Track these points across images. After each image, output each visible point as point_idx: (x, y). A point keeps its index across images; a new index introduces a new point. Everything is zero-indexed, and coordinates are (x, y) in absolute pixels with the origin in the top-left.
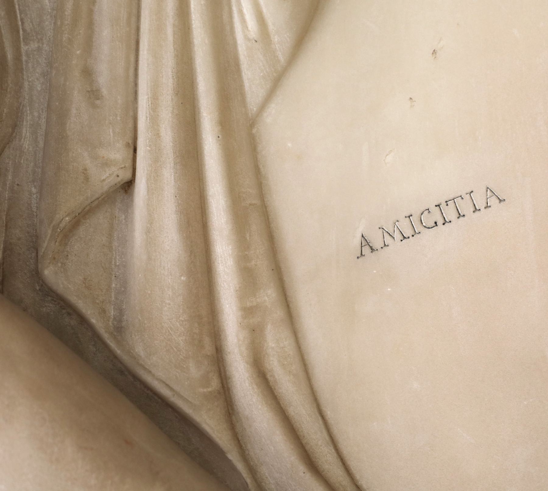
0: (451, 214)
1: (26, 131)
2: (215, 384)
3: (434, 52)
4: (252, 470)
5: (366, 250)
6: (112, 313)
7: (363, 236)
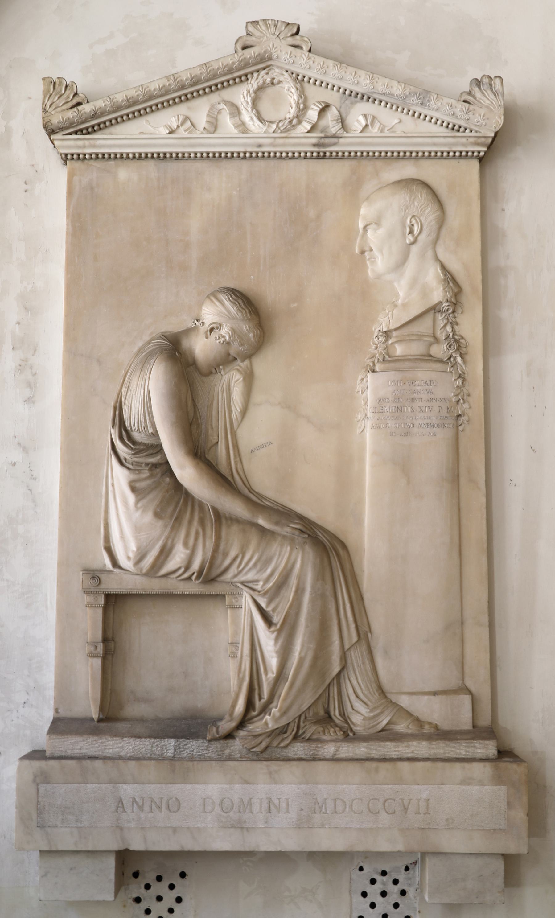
1: (202, 434)
2: (231, 473)
4: (236, 486)
6: (216, 462)
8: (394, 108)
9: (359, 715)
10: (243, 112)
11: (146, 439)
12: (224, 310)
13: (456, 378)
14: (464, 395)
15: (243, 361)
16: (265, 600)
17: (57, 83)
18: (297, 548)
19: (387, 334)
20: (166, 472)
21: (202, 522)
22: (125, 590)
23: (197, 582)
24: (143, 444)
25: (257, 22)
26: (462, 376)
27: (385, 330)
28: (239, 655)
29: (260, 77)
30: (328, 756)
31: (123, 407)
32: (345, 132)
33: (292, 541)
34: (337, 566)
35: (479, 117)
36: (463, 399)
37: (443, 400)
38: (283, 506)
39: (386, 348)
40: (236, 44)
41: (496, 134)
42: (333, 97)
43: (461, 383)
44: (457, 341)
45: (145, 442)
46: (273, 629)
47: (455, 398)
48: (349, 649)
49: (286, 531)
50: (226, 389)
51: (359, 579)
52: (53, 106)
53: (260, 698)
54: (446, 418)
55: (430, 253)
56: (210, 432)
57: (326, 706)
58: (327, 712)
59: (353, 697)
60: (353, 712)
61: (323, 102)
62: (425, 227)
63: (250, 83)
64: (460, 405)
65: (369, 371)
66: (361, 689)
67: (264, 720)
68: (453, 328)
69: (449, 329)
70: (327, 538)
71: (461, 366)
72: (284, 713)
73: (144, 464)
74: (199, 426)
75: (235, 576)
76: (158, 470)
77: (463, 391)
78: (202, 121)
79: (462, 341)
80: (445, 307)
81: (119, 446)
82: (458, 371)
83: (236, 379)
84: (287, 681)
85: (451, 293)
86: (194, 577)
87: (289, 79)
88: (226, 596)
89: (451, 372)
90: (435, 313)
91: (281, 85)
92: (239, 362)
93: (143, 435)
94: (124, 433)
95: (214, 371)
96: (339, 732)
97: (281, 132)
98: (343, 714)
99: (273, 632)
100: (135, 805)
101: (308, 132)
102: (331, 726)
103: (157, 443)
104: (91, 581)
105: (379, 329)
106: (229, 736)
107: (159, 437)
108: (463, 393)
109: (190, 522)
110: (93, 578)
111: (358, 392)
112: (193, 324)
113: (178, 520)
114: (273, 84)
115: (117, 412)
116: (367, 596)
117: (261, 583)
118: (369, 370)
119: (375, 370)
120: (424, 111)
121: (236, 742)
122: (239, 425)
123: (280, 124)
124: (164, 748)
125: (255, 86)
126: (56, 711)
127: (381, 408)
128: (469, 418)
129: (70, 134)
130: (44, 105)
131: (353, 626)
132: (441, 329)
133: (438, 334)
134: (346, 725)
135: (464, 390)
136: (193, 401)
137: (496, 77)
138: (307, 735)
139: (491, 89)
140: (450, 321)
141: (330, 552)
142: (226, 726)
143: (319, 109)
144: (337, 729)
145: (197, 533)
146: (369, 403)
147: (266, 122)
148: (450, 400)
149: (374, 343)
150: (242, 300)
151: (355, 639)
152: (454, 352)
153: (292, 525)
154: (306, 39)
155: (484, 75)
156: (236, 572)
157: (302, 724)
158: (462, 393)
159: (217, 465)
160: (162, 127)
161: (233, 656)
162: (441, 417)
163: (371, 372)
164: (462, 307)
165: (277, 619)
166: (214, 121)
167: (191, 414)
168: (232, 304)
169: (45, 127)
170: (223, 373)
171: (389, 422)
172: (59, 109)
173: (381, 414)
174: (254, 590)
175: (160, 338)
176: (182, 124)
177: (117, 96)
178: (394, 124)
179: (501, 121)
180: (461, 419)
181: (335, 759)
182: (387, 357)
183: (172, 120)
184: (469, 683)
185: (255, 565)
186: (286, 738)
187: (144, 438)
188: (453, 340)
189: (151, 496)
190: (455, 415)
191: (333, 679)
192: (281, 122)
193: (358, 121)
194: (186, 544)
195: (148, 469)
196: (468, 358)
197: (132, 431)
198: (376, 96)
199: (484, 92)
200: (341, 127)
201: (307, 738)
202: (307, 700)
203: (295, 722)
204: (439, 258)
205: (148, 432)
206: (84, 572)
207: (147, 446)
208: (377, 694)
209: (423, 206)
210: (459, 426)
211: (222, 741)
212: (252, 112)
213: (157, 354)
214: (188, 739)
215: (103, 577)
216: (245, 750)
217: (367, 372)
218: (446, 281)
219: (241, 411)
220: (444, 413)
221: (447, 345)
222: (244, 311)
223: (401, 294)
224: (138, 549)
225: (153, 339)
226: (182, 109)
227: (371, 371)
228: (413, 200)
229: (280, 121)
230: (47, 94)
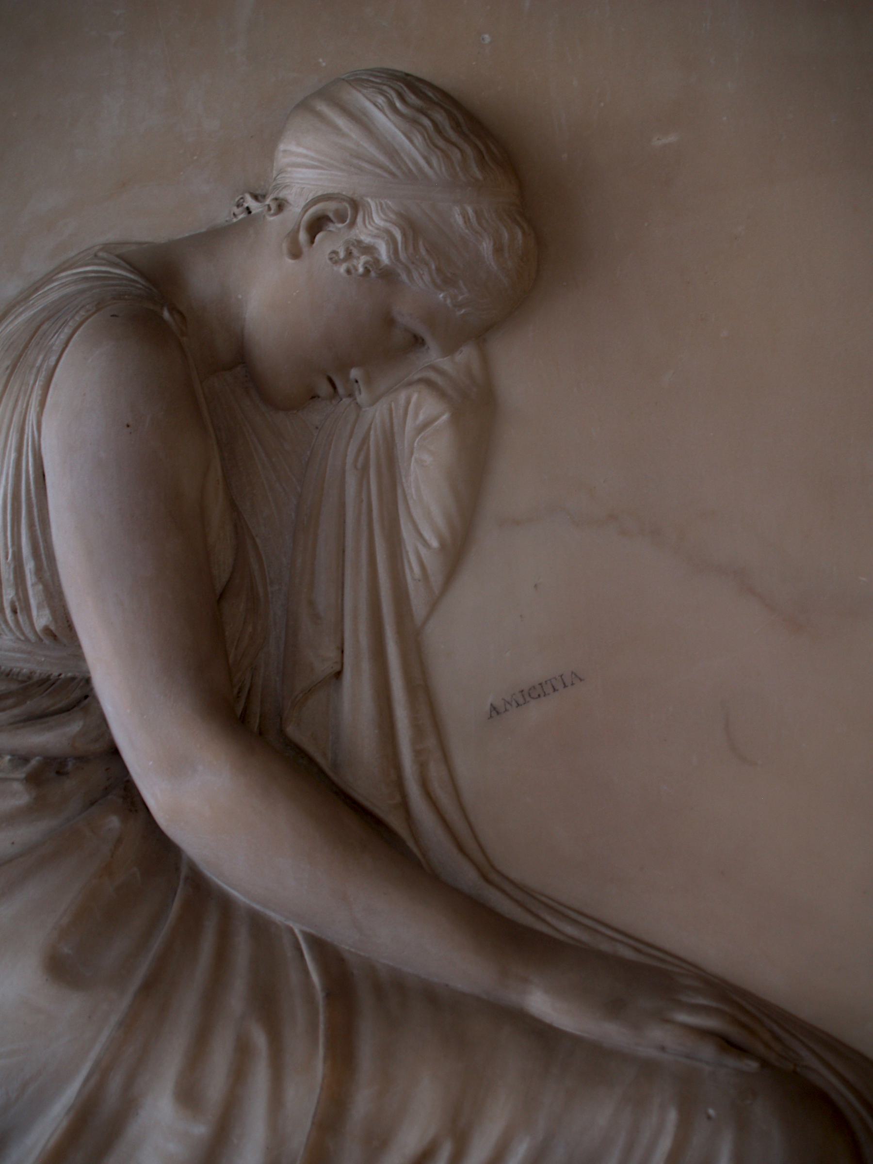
0: (548, 689)
3: (536, 586)
5: (494, 713)
7: (491, 705)
11: (18, 655)
12: (370, 148)
15: (449, 350)
18: (709, 1117)
20: (107, 791)
24: (8, 675)
45: (16, 670)
73: (8, 758)
76: (69, 784)
83: (421, 417)
92: (433, 355)
95: (324, 388)
103: (69, 675)
107: (79, 647)
112: (236, 210)
122: (434, 606)
136: (233, 506)
153: (683, 1017)
170: (363, 397)
187: (13, 650)
195: (23, 776)
205: (32, 625)
213: (82, 313)
219: (443, 545)
222: (456, 151)
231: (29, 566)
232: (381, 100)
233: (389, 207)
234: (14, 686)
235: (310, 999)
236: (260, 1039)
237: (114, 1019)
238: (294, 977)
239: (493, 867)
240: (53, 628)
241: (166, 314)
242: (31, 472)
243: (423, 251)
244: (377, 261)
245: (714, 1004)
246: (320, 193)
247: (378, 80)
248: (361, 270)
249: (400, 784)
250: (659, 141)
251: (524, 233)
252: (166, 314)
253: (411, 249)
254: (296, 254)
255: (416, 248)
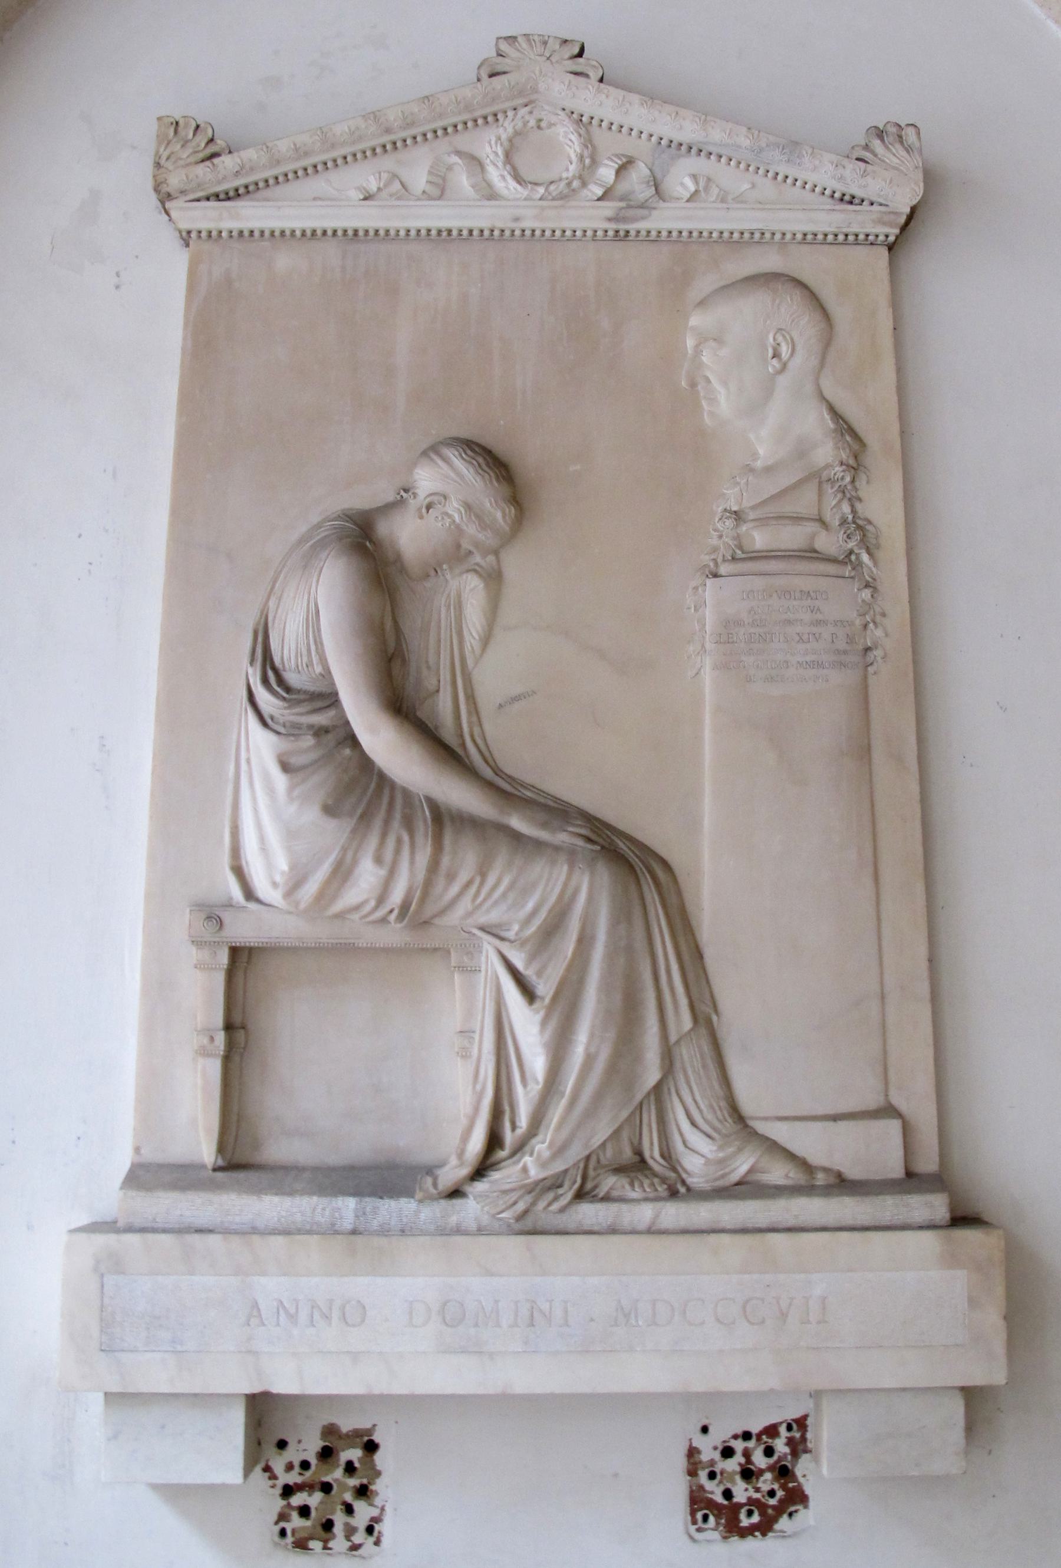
0: (522, 698)
8: (742, 166)
9: (696, 1155)
10: (490, 169)
11: (308, 684)
13: (861, 587)
14: (874, 615)
16: (523, 955)
17: (181, 123)
18: (580, 868)
19: (738, 516)
21: (409, 824)
22: (266, 940)
23: (399, 926)
25: (515, 38)
26: (871, 585)
27: (735, 508)
28: (475, 1052)
29: (519, 116)
30: (642, 1226)
31: (270, 631)
32: (661, 201)
33: (572, 854)
34: (653, 898)
35: (884, 183)
36: (875, 623)
37: (839, 624)
38: (556, 799)
39: (738, 538)
40: (479, 68)
41: (913, 210)
42: (641, 148)
43: (869, 595)
44: (860, 528)
45: (308, 690)
46: (537, 1005)
47: (861, 620)
48: (678, 1042)
49: (562, 838)
50: (454, 601)
51: (694, 923)
52: (173, 159)
53: (514, 1127)
54: (845, 652)
55: (809, 388)
56: (425, 672)
57: (636, 1142)
58: (639, 1153)
59: (685, 1125)
60: (687, 1151)
61: (623, 155)
62: (799, 348)
63: (502, 126)
64: (868, 632)
65: (707, 576)
66: (701, 1111)
67: (521, 1165)
68: (852, 506)
69: (846, 508)
70: (638, 853)
71: (870, 569)
72: (559, 1151)
74: (404, 662)
75: (469, 914)
76: (330, 736)
77: (873, 608)
78: (419, 179)
79: (869, 527)
80: (838, 474)
81: (263, 696)
82: (864, 576)
83: (472, 585)
84: (563, 1097)
85: (848, 450)
86: (393, 917)
87: (567, 120)
88: (452, 950)
89: (852, 578)
90: (820, 483)
91: (553, 128)
93: (304, 678)
94: (271, 674)
95: (432, 573)
96: (661, 1186)
97: (553, 199)
98: (667, 1155)
99: (537, 1012)
100: (282, 1312)
101: (599, 199)
102: (646, 1177)
104: (205, 924)
105: (725, 507)
106: (456, 1193)
108: (874, 611)
109: (387, 822)
110: (209, 918)
111: (689, 608)
113: (365, 818)
114: (539, 127)
115: (260, 639)
116: (709, 953)
117: (516, 927)
118: (707, 573)
119: (719, 574)
120: (792, 173)
121: (469, 1201)
122: (476, 663)
123: (552, 187)
124: (336, 1213)
125: (510, 130)
126: (137, 1150)
127: (730, 636)
128: (885, 653)
129: (198, 200)
130: (158, 158)
131: (684, 1002)
132: (832, 509)
133: (828, 516)
134: (673, 1175)
135: (876, 607)
137: (908, 125)
138: (602, 1191)
139: (902, 143)
140: (848, 495)
141: (640, 874)
142: (453, 1173)
143: (616, 166)
144: (656, 1181)
145: (399, 841)
146: (708, 628)
147: (529, 184)
148: (851, 624)
149: (715, 530)
150: (485, 459)
151: (687, 1023)
152: (857, 545)
153: (571, 829)
154: (594, 63)
155: (888, 122)
156: (470, 907)
157: (591, 1173)
158: (872, 612)
159: (436, 728)
160: (354, 190)
161: (464, 1054)
162: (836, 652)
163: (711, 577)
164: (868, 474)
165: (545, 989)
166: (441, 182)
167: (392, 644)
168: (467, 465)
169: (157, 189)
171: (743, 658)
172: (181, 162)
173: (728, 645)
174: (502, 939)
175: (338, 518)
176: (386, 186)
177: (278, 143)
178: (743, 189)
179: (920, 192)
180: (871, 656)
181: (652, 1231)
182: (739, 552)
183: (370, 180)
184: (898, 1101)
185: (504, 895)
186: (562, 1195)
188: (854, 526)
189: (315, 779)
190: (862, 648)
191: (648, 1094)
192: (553, 184)
193: (682, 184)
194: (378, 860)
195: (312, 733)
196: (880, 555)
197: (285, 670)
198: (711, 149)
199: (890, 146)
200: (654, 192)
201: (601, 1195)
202: (602, 1131)
203: (579, 1167)
204: (826, 397)
205: (314, 672)
206: (193, 908)
207: (311, 695)
208: (730, 1120)
209: (794, 316)
210: (868, 666)
211: (444, 1203)
212: (505, 168)
214: (381, 1198)
215: (227, 917)
216: (486, 1217)
217: (704, 577)
218: (840, 433)
220: (841, 645)
221: (843, 535)
223: (761, 452)
224: (293, 867)
225: (325, 520)
226: (388, 163)
227: (712, 575)
228: (779, 305)
229: (552, 182)
230: (162, 140)
231: (313, 647)
232: (456, 453)
233: (460, 500)
234: (307, 697)
235: (425, 820)
236: (406, 838)
237: (348, 830)
238: (419, 814)
239: (498, 767)
240: (323, 673)
241: (368, 544)
242: (313, 609)
243: (473, 518)
244: (454, 521)
245: (584, 824)
246: (431, 492)
247: (455, 444)
248: (448, 525)
249: (461, 736)
250: (572, 468)
251: (515, 508)
252: (368, 544)
253: (468, 517)
254: (421, 517)
255: (470, 516)
